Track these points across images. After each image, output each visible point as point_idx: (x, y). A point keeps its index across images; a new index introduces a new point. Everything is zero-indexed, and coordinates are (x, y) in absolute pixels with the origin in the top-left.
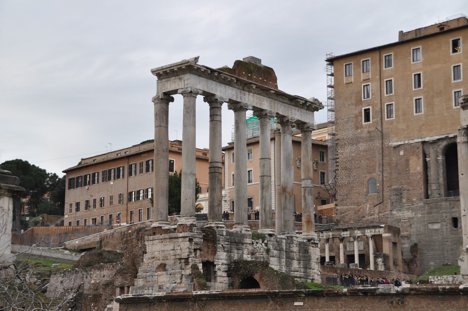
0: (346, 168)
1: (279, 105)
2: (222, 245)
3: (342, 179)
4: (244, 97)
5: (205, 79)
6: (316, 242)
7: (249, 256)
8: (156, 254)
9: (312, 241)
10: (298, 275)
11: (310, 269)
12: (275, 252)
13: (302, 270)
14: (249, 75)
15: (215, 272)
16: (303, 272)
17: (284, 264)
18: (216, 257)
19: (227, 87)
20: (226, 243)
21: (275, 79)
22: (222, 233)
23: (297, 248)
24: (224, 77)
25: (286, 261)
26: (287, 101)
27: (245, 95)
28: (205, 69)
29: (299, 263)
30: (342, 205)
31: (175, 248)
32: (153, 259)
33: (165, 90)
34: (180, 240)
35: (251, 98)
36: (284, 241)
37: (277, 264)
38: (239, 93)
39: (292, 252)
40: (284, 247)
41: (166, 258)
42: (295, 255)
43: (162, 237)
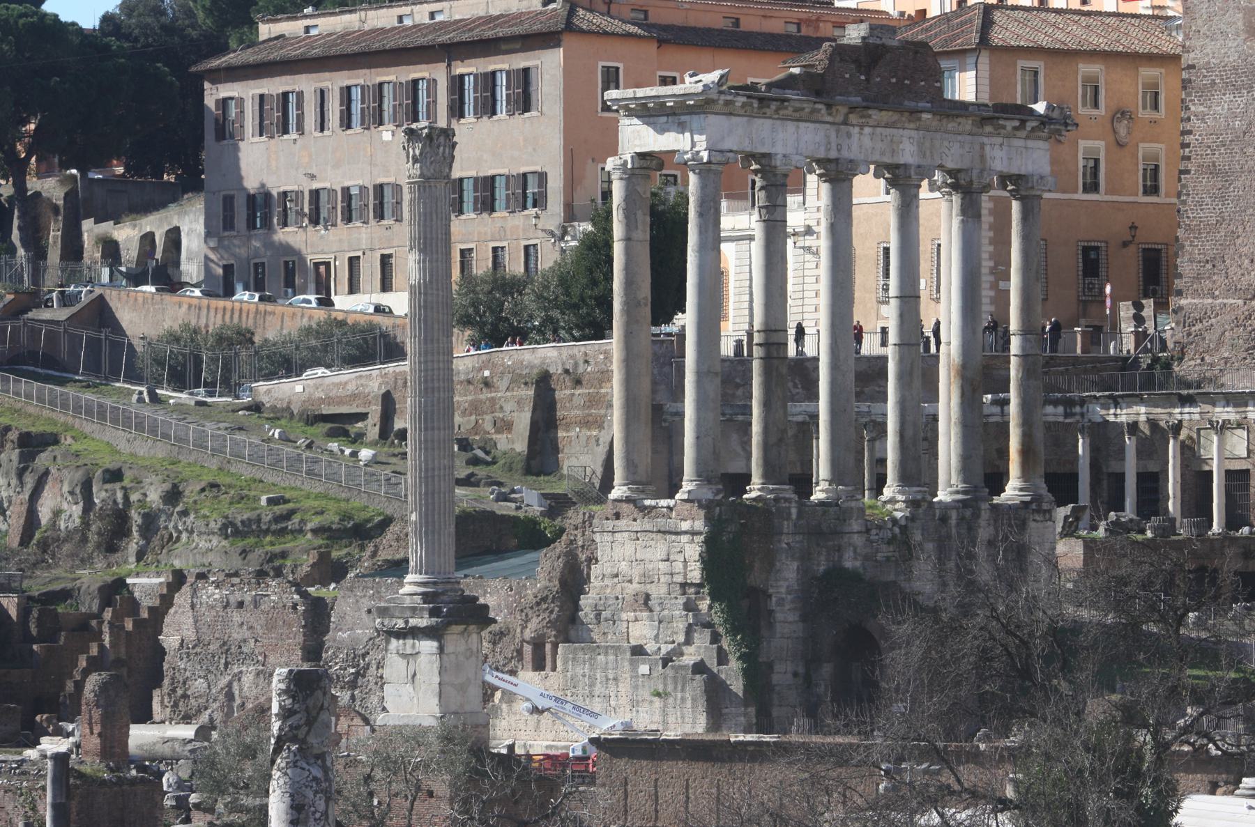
0: (1213, 170)
1: (946, 143)
3: (1200, 203)
5: (745, 119)
8: (624, 566)
15: (771, 612)
19: (802, 125)
20: (798, 538)
27: (849, 135)
30: (1196, 293)
31: (672, 557)
32: (616, 580)
33: (640, 146)
34: (685, 538)
35: (867, 141)
38: (833, 135)
41: (647, 578)
43: (636, 526)
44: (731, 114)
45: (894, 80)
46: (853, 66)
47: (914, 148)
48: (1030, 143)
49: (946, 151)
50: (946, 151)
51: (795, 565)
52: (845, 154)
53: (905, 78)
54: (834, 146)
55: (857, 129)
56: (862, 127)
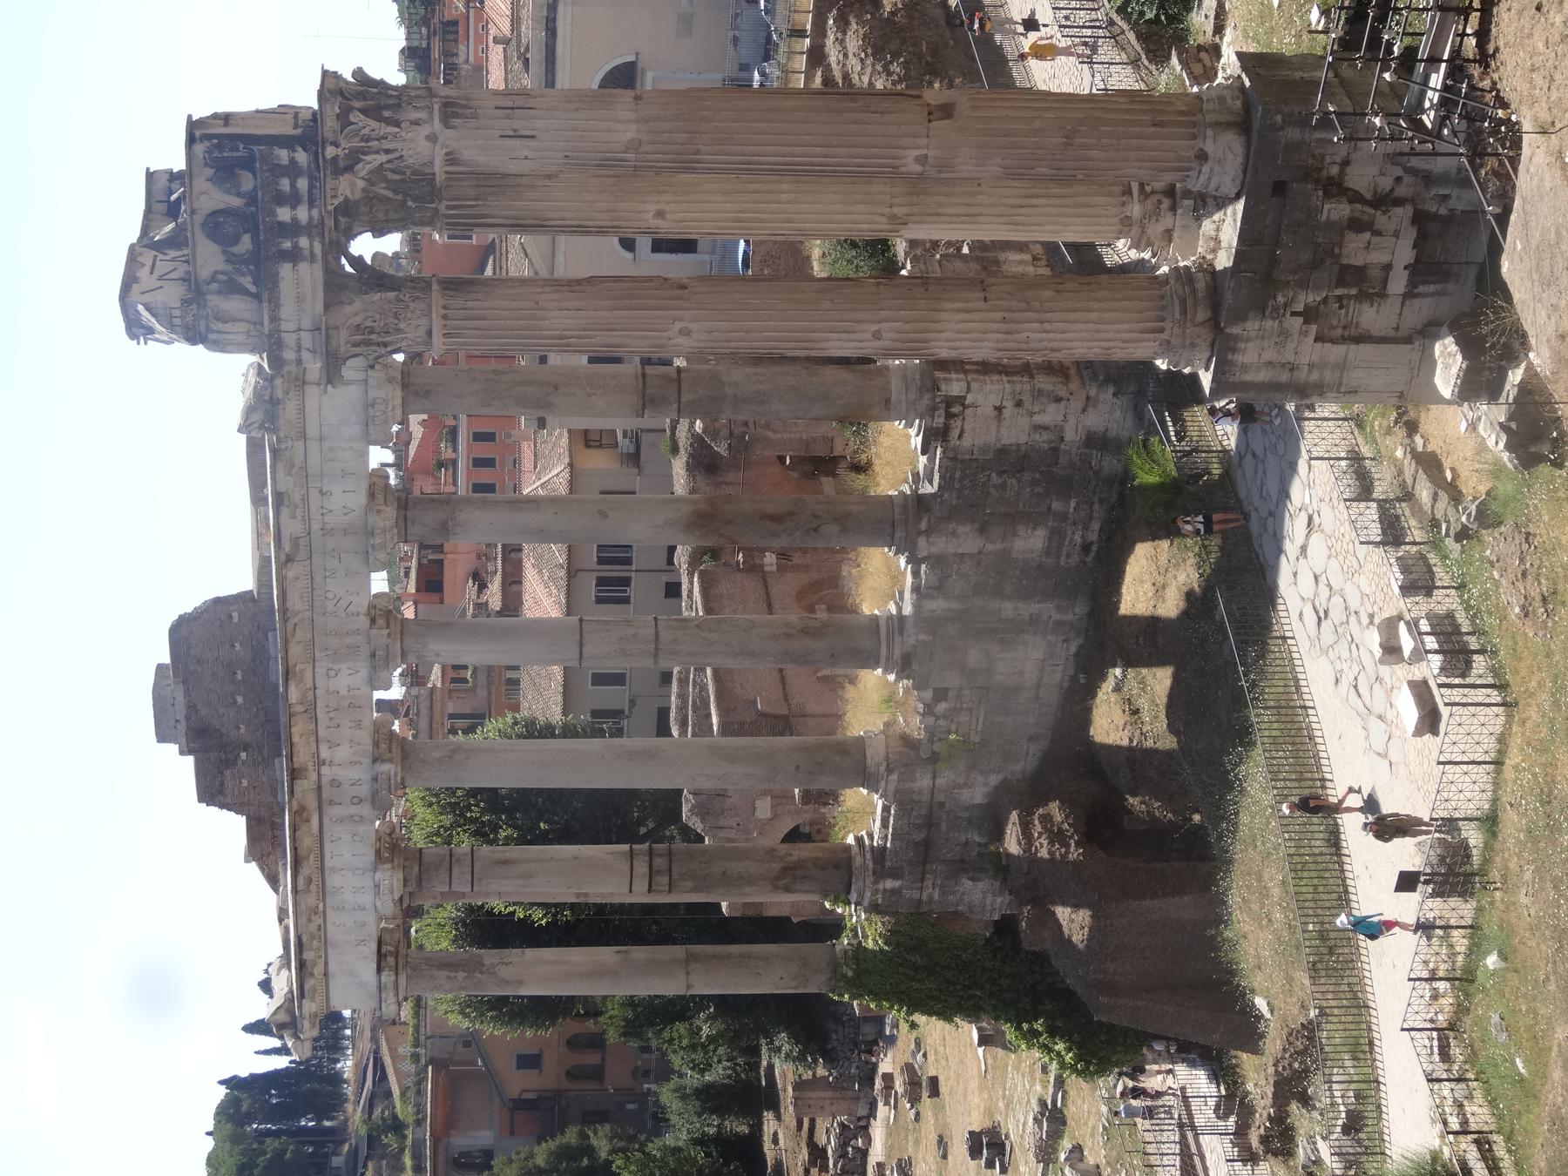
1: (330, 606)
5: (330, 951)
10: (1078, 538)
11: (1055, 451)
12: (974, 657)
13: (1056, 505)
14: (243, 755)
17: (1021, 605)
19: (328, 863)
23: (964, 529)
27: (336, 784)
29: (1032, 520)
35: (343, 753)
38: (336, 811)
40: (955, 605)
42: (990, 547)
44: (326, 974)
45: (240, 700)
46: (228, 773)
47: (343, 666)
48: (312, 431)
49: (343, 604)
50: (343, 604)
51: (967, 884)
52: (364, 790)
54: (355, 810)
55: (325, 770)
56: (321, 763)
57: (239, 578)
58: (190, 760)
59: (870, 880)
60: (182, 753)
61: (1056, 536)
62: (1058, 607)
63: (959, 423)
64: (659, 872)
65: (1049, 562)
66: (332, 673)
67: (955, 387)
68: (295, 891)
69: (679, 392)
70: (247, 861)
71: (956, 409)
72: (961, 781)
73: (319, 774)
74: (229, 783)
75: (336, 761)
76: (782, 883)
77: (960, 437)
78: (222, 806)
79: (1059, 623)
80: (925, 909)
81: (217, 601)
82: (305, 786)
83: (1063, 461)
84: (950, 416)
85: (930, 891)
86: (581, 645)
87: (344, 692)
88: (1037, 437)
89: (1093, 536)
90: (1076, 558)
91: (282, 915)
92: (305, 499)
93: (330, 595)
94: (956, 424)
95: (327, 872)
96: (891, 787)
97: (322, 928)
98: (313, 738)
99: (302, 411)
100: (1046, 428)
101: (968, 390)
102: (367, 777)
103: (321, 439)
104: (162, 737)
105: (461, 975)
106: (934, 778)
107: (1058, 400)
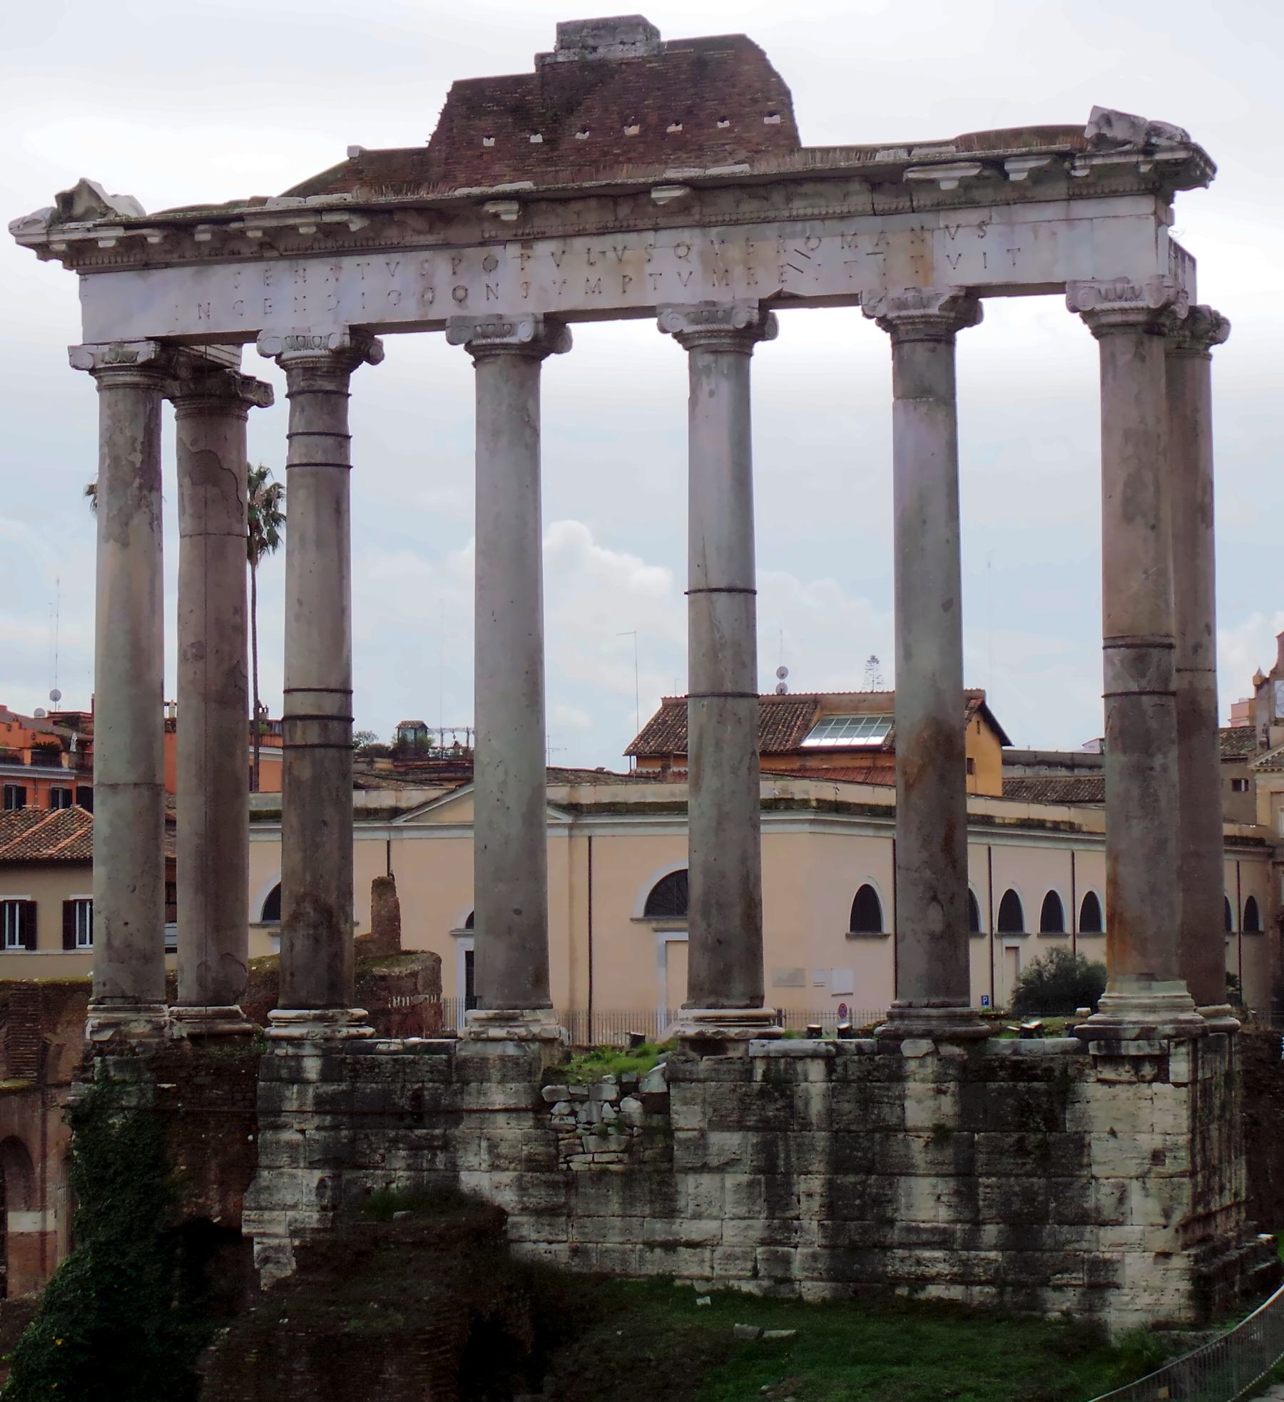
2: (302, 1132)
4: (486, 279)
5: (188, 271)
6: (1131, 1049)
7: (506, 1177)
9: (1092, 1049)
10: (943, 1268)
12: (727, 1142)
13: (991, 1232)
14: (537, 139)
16: (995, 1248)
17: (816, 1204)
18: (248, 1200)
19: (349, 263)
20: (317, 1121)
21: (775, 95)
22: (300, 1069)
23: (948, 1105)
24: (266, 231)
25: (830, 1185)
26: (860, 198)
27: (490, 265)
28: (120, 232)
29: (966, 1195)
36: (816, 1070)
37: (742, 1210)
39: (902, 1127)
40: (816, 1107)
42: (917, 1145)
45: (633, 130)
47: (694, 263)
48: (1082, 208)
50: (799, 261)
52: (479, 307)
53: (666, 123)
55: (513, 250)
57: (823, 123)
58: (530, 68)
59: (319, 1030)
60: (541, 59)
61: (942, 1239)
62: (814, 1257)
63: (1125, 1077)
64: (325, 729)
65: (895, 1235)
66: (682, 251)
67: (1180, 1067)
68: (318, 211)
69: (1153, 693)
70: (350, 149)
71: (1148, 1070)
72: (504, 1149)
73: (504, 243)
74: (486, 123)
75: (529, 265)
76: (308, 908)
77: (1099, 1081)
78: (447, 114)
79: (786, 1261)
80: (261, 1122)
81: (787, 94)
82: (510, 212)
83: (1066, 1232)
84: (1137, 1061)
85: (300, 1128)
86: (729, 590)
87: (649, 268)
88: (1106, 1190)
89: (934, 1291)
90: (904, 1269)
91: (263, 201)
92: (973, 204)
93: (813, 243)
94: (1125, 1073)
95: (333, 260)
96: (494, 1051)
97: (235, 257)
98: (569, 229)
99: (1115, 194)
100: (1122, 1200)
101: (1177, 1085)
102: (500, 308)
103: (1069, 220)
104: (567, 32)
105: (138, 458)
106: (506, 1110)
107: (1167, 1214)
